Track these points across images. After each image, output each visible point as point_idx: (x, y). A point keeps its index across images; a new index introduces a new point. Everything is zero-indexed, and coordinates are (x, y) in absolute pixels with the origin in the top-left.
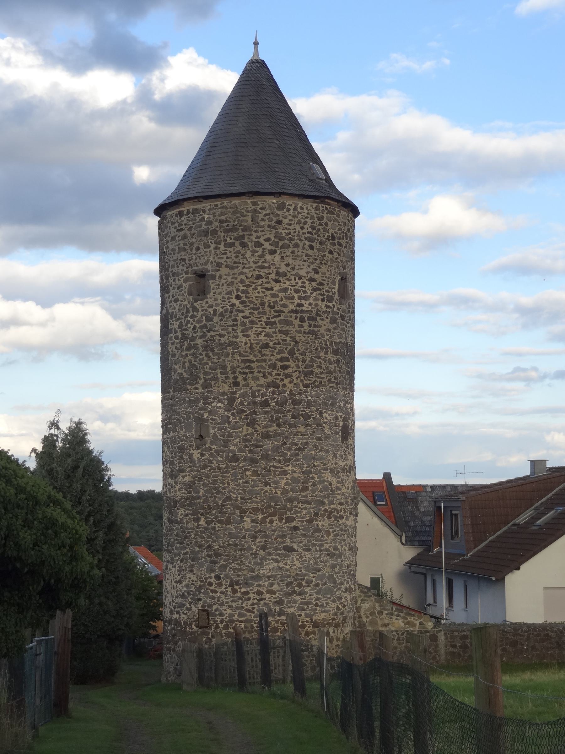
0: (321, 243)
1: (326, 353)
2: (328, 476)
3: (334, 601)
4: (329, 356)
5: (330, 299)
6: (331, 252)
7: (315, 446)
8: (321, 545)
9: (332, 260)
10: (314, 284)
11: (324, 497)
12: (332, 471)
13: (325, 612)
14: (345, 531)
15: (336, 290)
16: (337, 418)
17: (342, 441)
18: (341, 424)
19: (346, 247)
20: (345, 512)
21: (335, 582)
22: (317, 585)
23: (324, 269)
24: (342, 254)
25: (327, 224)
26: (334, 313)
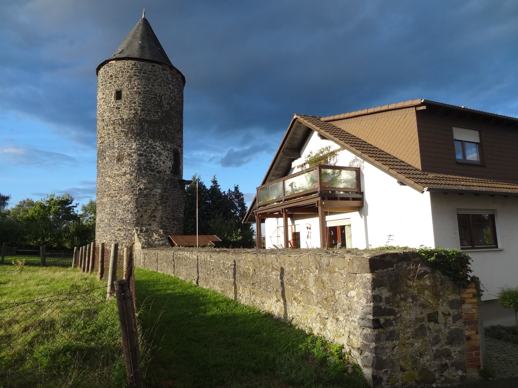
0: (105, 82)
1: (107, 126)
2: (108, 179)
3: (110, 234)
4: (109, 127)
5: (109, 103)
6: (110, 83)
7: (103, 168)
8: (105, 210)
9: (111, 86)
10: (103, 100)
11: (106, 189)
12: (109, 177)
13: (105, 239)
14: (119, 203)
15: (113, 98)
16: (114, 153)
17: (117, 162)
18: (117, 155)
19: (122, 77)
20: (118, 193)
21: (110, 226)
22: (102, 228)
23: (107, 91)
24: (118, 81)
25: (108, 72)
26: (111, 108)
